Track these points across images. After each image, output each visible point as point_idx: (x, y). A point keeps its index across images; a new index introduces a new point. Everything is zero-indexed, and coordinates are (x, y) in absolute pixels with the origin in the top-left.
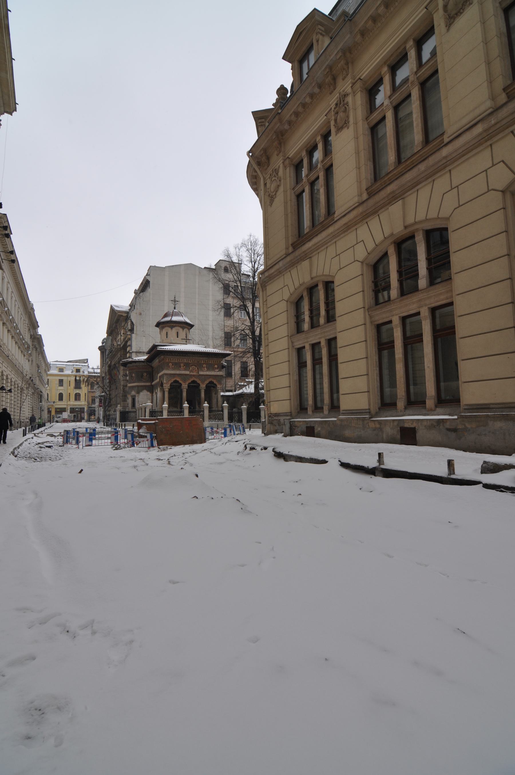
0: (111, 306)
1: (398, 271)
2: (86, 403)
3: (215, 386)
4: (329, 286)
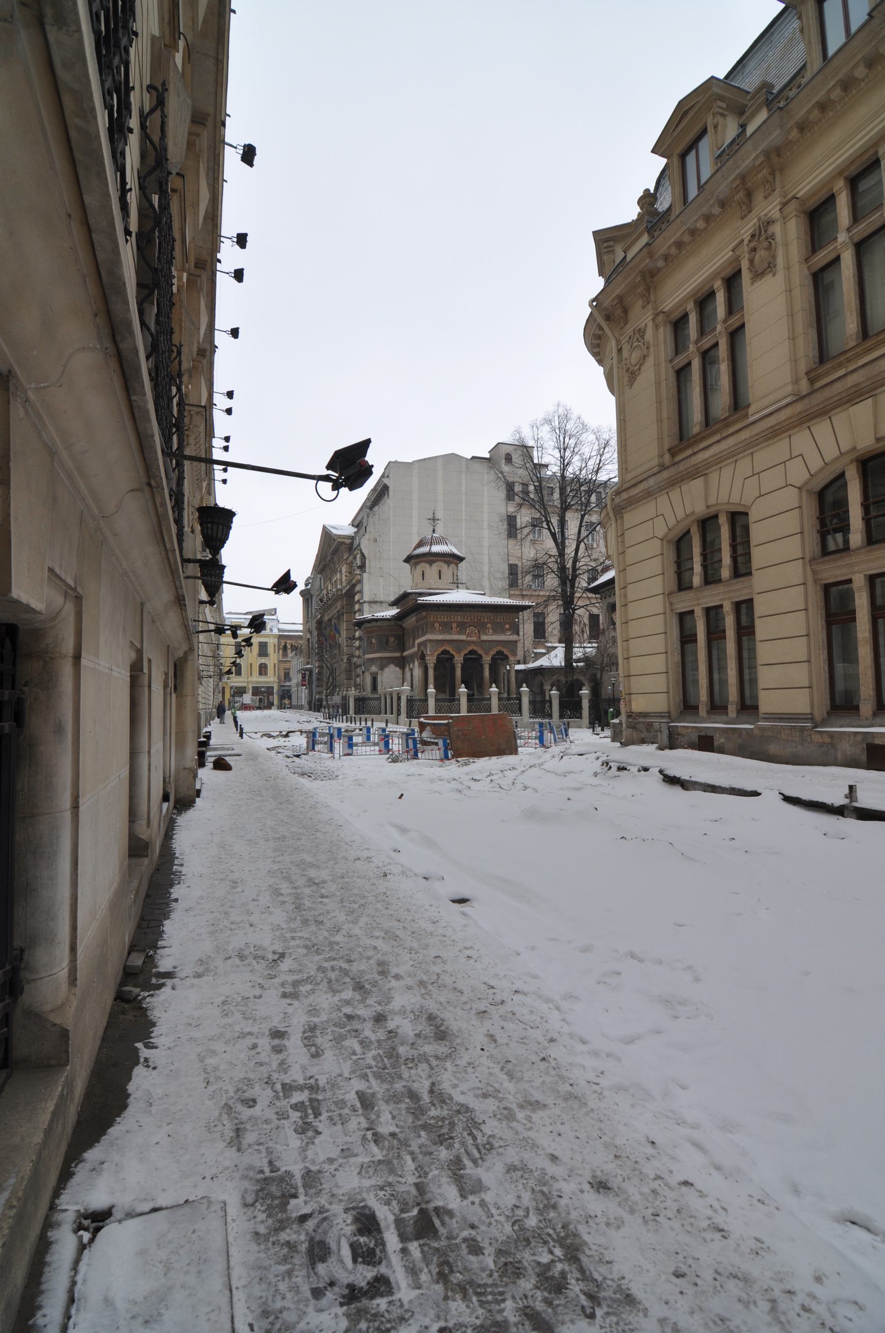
0: (324, 527)
1: (862, 505)
2: (276, 680)
3: (505, 658)
4: (739, 519)
